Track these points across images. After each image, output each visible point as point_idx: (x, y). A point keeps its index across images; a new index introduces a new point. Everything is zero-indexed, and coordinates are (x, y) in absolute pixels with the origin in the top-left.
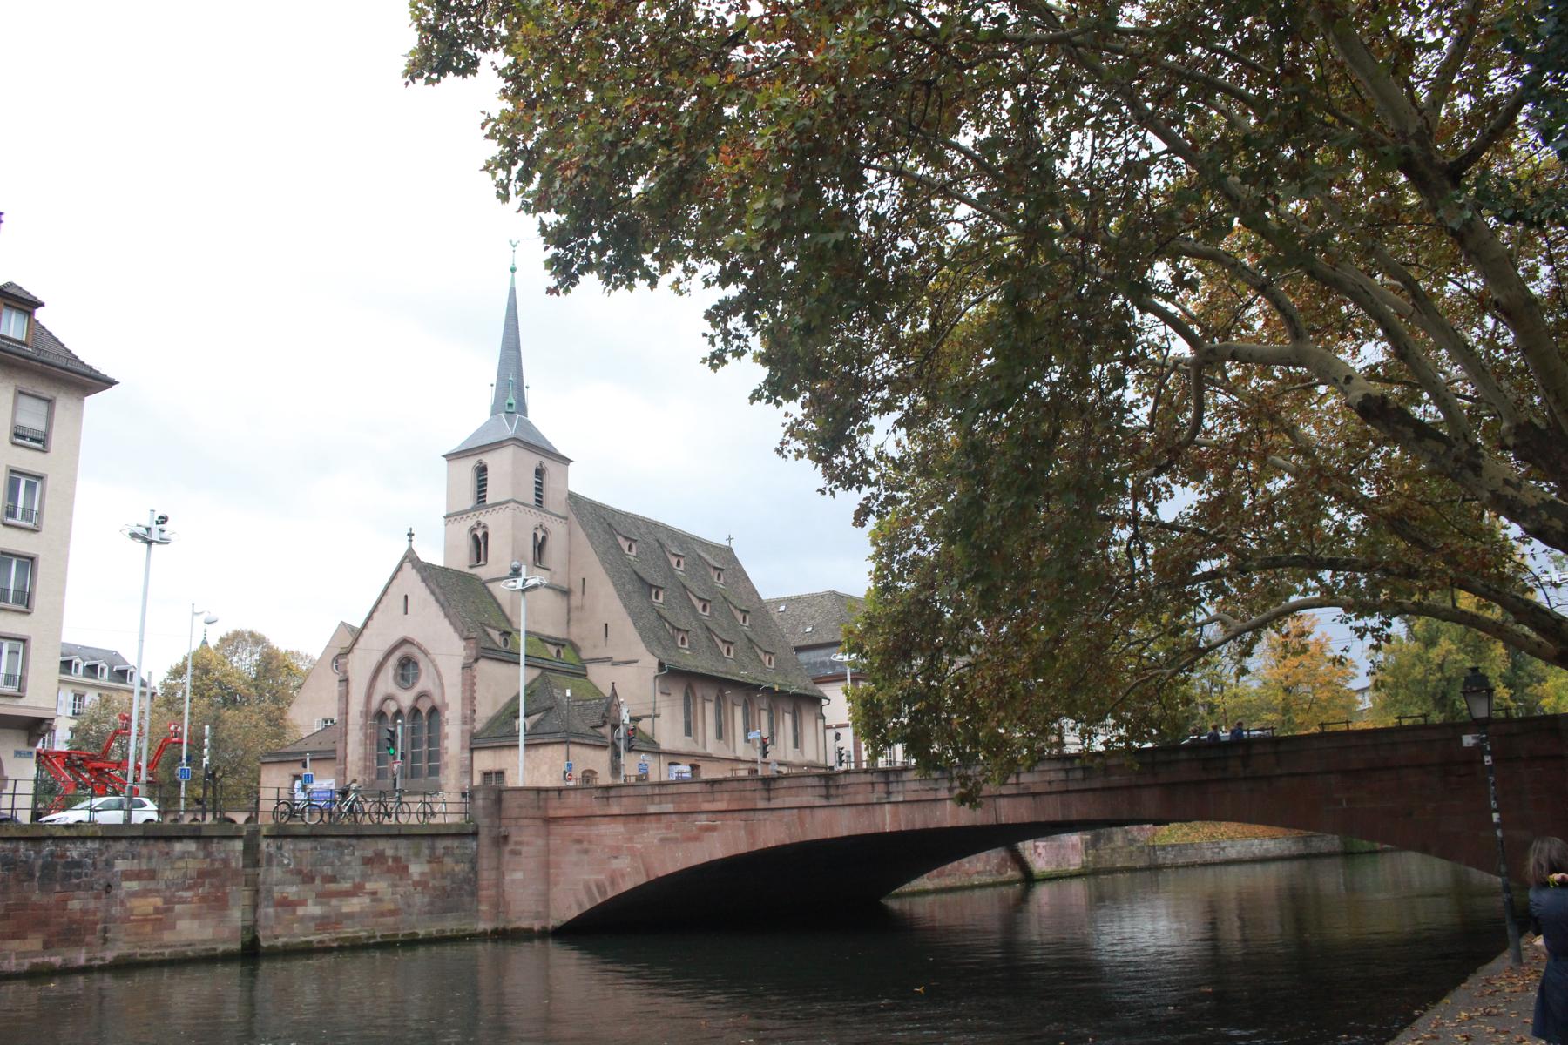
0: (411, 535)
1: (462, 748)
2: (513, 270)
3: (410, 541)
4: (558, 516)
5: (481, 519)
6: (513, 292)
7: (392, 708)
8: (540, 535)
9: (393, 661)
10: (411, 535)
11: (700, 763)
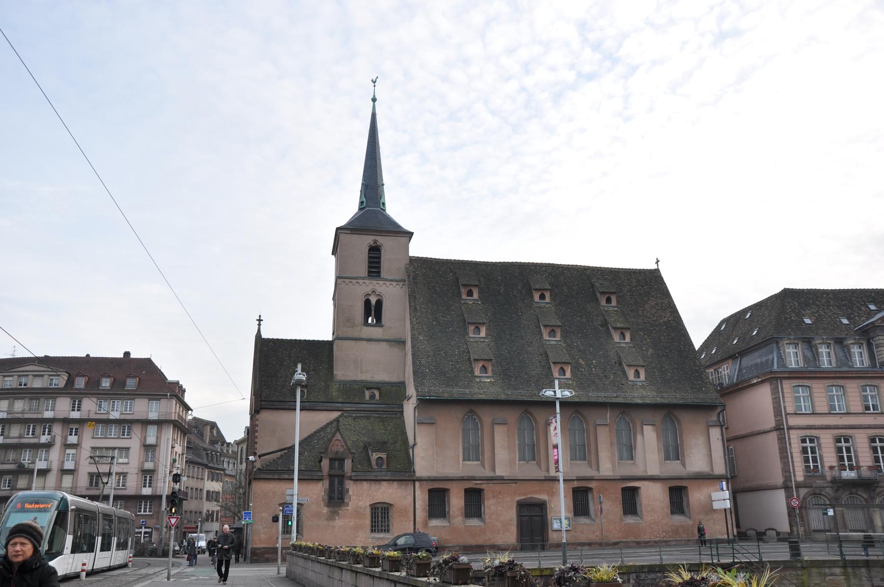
0: (260, 320)
2: (374, 100)
3: (259, 325)
4: (391, 281)
6: (374, 116)
8: (373, 300)
10: (260, 320)
11: (482, 487)
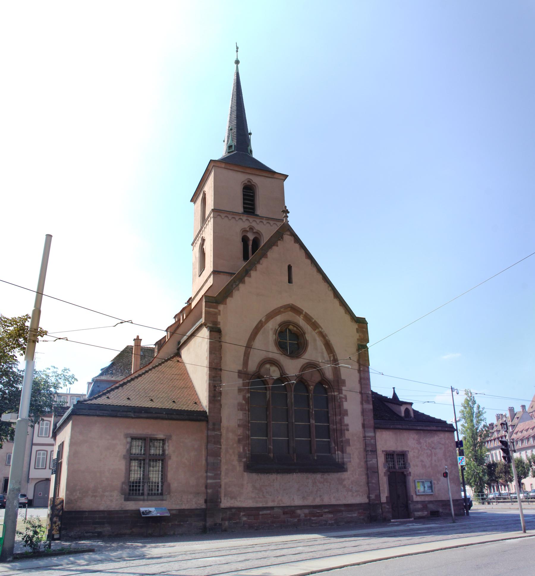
1: (364, 426)
2: (237, 62)
5: (254, 224)
7: (275, 373)
9: (273, 325)
